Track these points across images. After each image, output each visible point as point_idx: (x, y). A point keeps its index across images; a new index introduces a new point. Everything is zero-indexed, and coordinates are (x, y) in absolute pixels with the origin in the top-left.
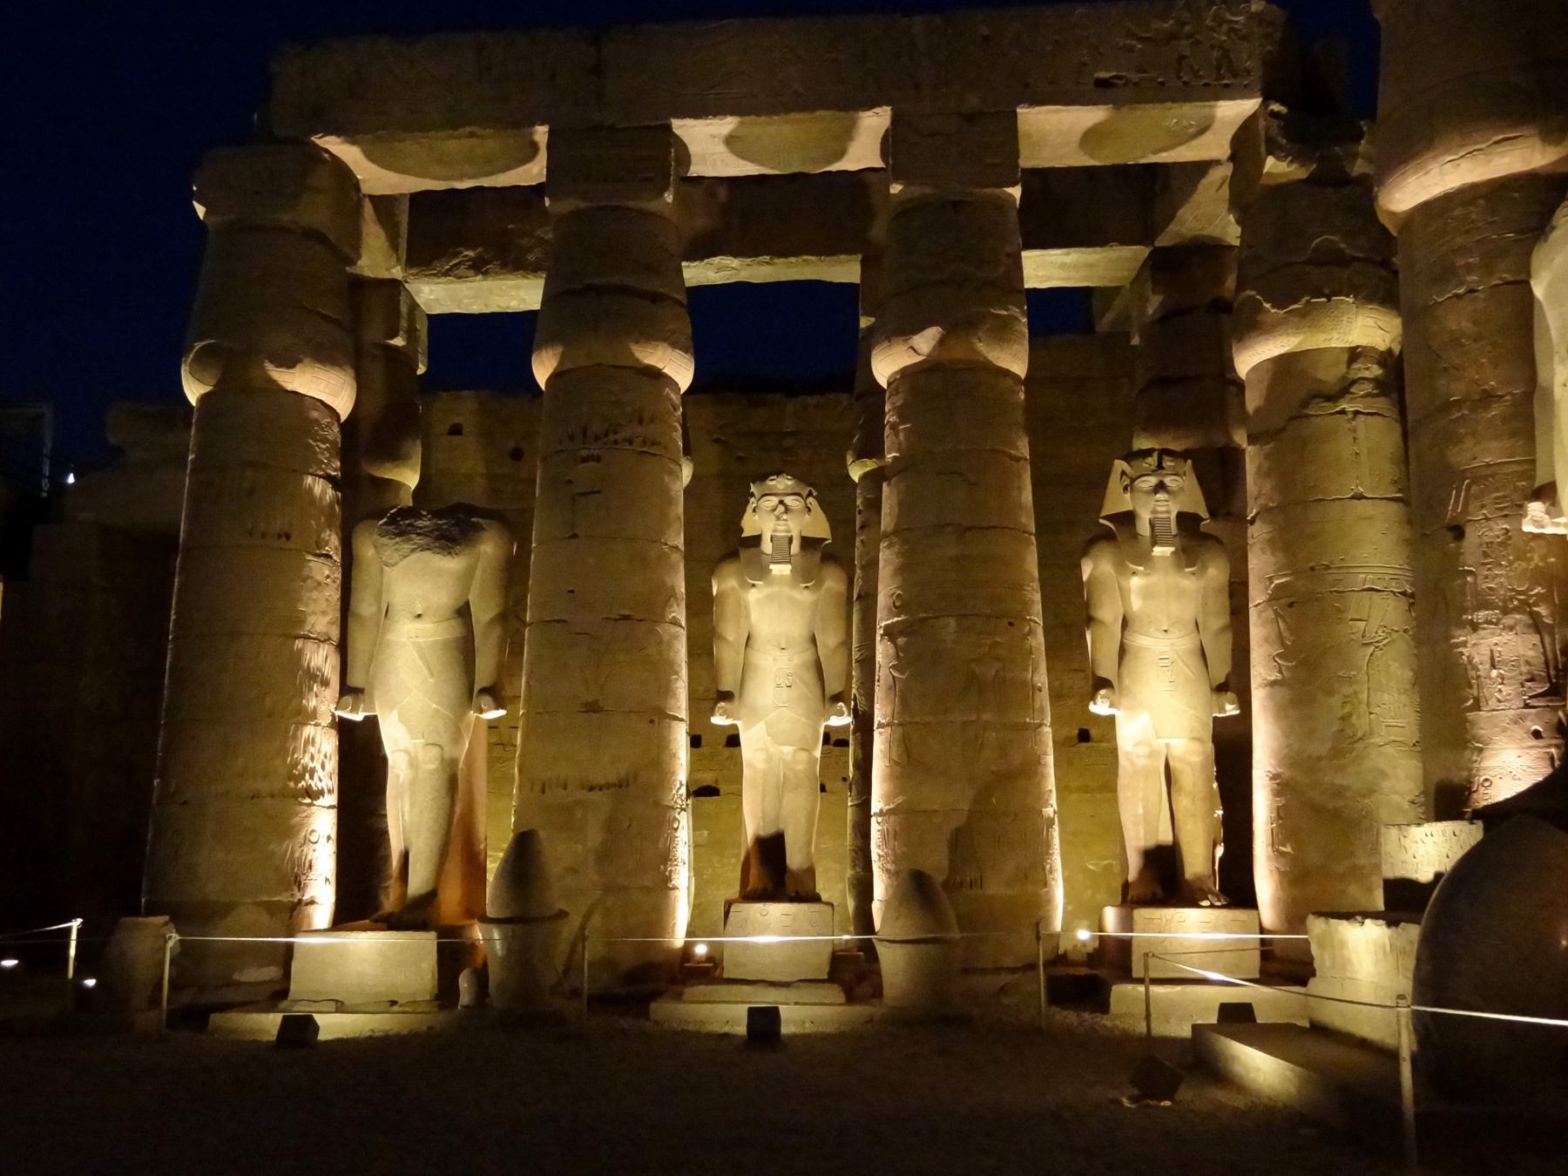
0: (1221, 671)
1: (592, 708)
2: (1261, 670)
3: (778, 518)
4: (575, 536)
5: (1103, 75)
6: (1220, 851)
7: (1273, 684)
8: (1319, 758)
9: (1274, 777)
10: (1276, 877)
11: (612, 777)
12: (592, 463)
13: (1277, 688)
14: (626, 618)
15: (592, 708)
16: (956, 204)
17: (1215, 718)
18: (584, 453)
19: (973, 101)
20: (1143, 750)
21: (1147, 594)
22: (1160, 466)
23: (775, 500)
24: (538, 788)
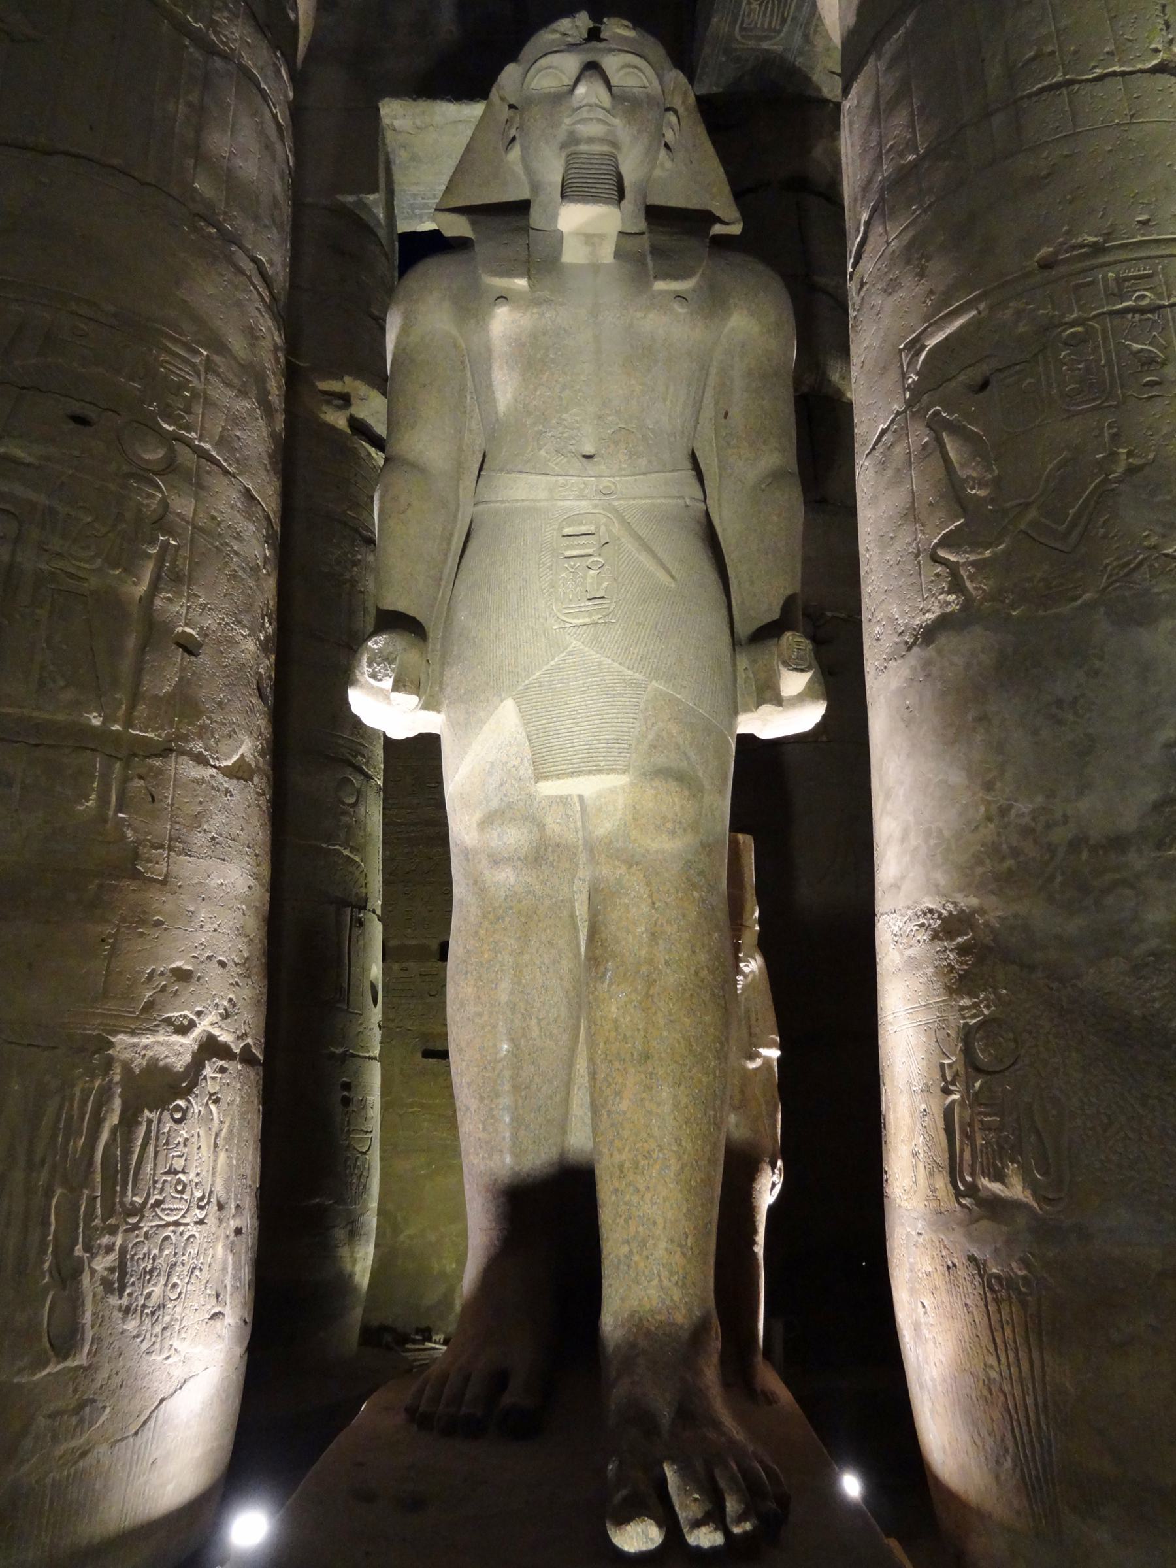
0: (764, 589)
2: (892, 601)
6: (768, 1189)
7: (928, 635)
8: (1118, 843)
9: (948, 928)
10: (971, 1292)
13: (942, 639)
17: (747, 742)
20: (513, 837)
21: (534, 357)
22: (594, 35)
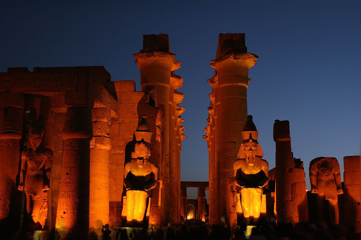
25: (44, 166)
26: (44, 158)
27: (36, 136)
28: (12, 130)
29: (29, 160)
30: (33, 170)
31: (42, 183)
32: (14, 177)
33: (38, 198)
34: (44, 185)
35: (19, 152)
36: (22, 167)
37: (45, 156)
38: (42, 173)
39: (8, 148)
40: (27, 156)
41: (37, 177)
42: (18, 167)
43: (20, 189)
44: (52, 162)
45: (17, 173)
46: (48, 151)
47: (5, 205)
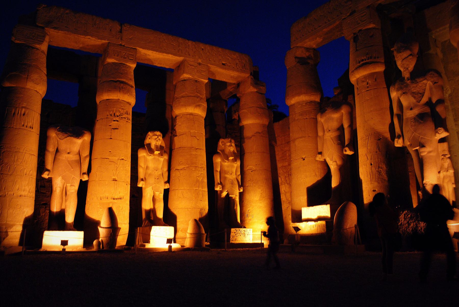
1: (115, 180)
3: (157, 141)
4: (111, 138)
5: (224, 62)
11: (119, 197)
12: (116, 122)
14: (123, 159)
15: (115, 180)
16: (196, 81)
18: (114, 119)
19: (200, 61)
23: (156, 137)
24: (99, 199)
25: (430, 99)
26: (426, 84)
27: (405, 54)
28: (368, 59)
29: (401, 95)
30: (411, 109)
31: (431, 125)
32: (384, 130)
33: (430, 152)
34: (436, 127)
35: (386, 89)
36: (395, 111)
37: (428, 81)
38: (428, 110)
39: (368, 87)
40: (398, 90)
41: (421, 118)
42: (388, 112)
43: (398, 143)
44: (443, 88)
45: (388, 121)
46: (431, 72)
47: (379, 173)
